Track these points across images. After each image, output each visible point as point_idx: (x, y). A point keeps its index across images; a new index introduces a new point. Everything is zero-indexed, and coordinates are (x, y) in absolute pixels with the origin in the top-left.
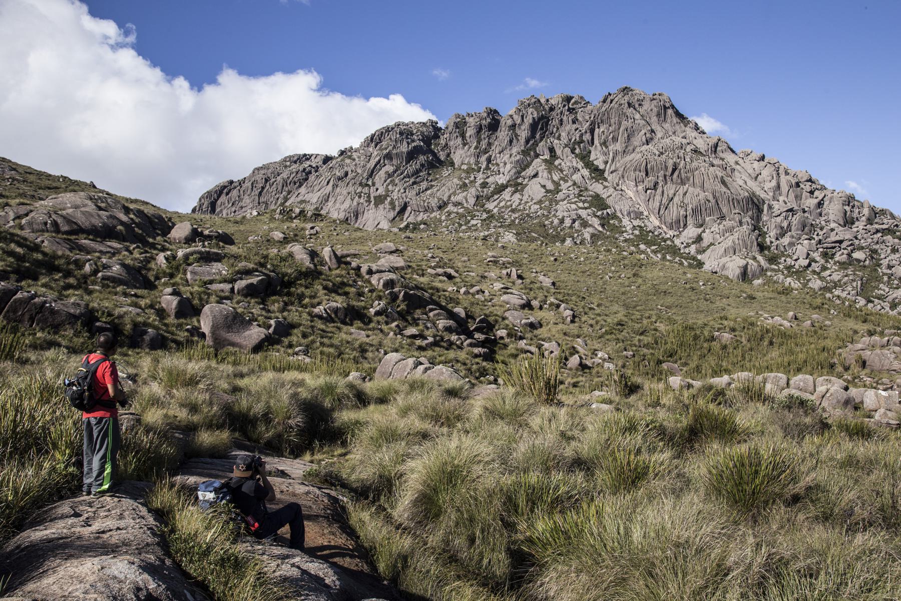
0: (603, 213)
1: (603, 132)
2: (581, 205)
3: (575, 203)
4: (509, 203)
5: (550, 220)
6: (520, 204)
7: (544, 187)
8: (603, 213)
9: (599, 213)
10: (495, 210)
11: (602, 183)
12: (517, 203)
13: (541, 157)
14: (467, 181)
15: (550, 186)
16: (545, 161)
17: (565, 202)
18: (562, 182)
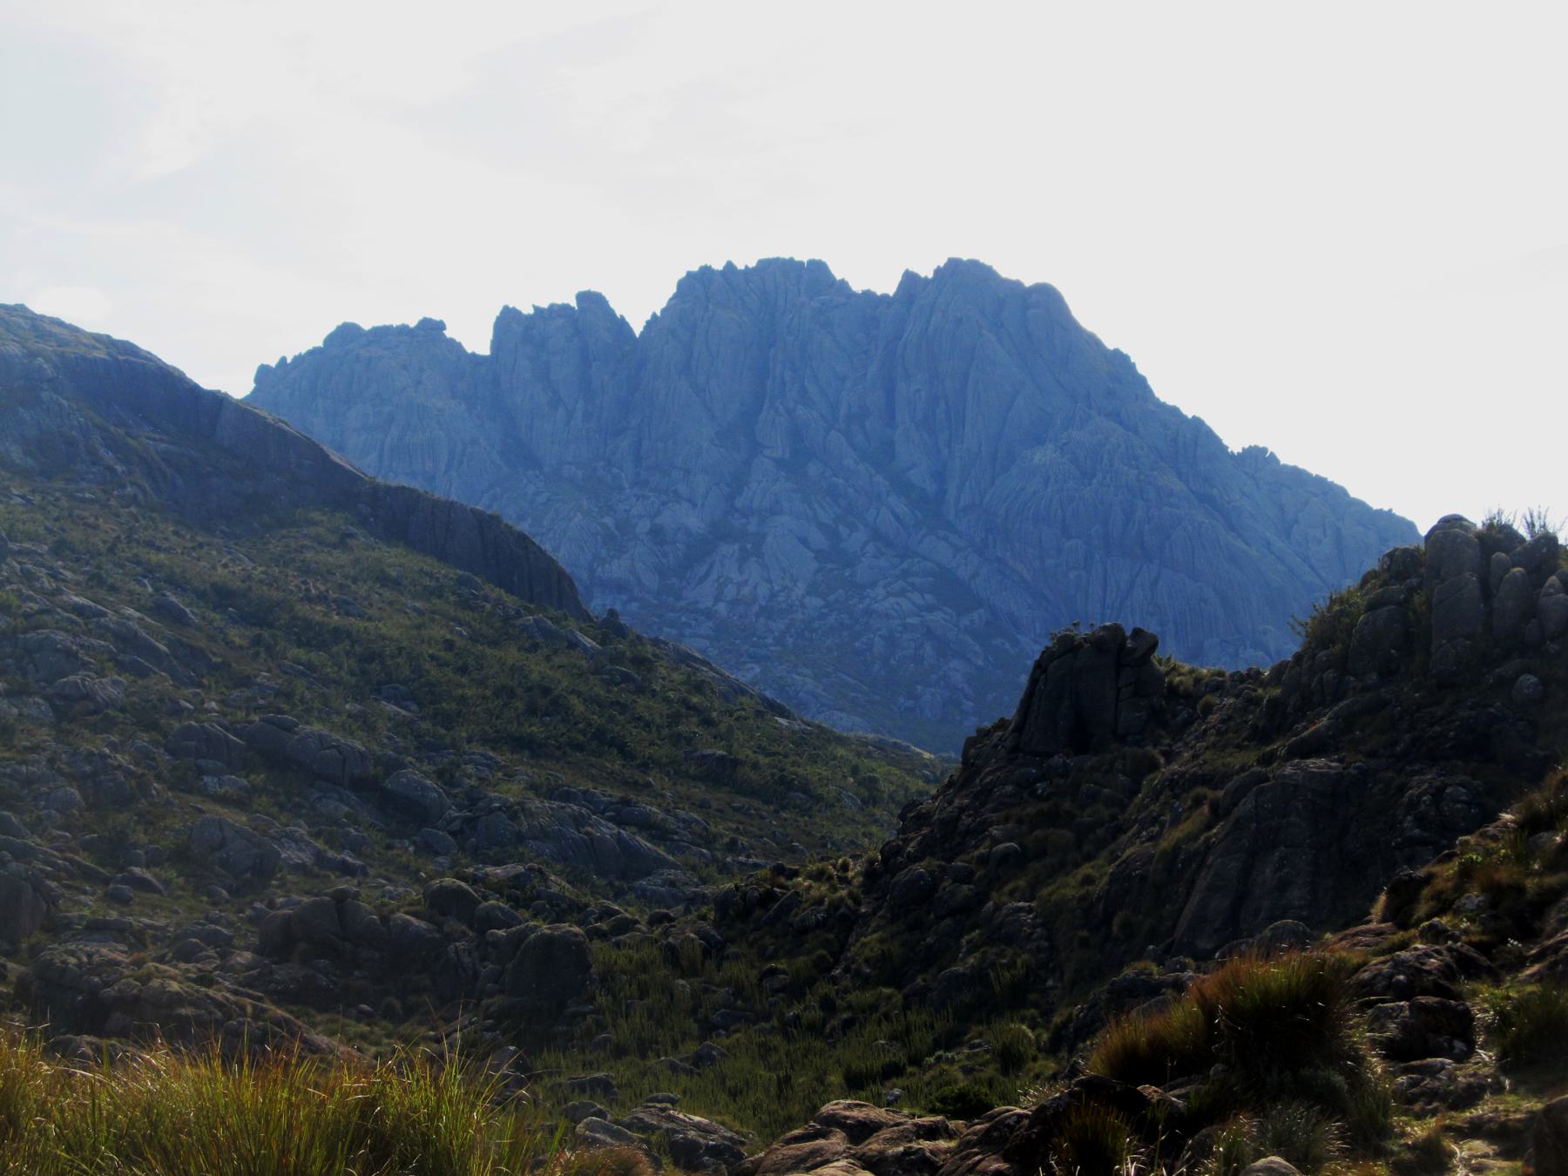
0: (972, 622)
1: (918, 390)
2: (916, 597)
3: (902, 593)
4: (746, 591)
5: (864, 639)
6: (773, 595)
7: (804, 541)
8: (972, 622)
9: (965, 621)
10: (722, 608)
11: (946, 539)
12: (763, 590)
13: (767, 452)
14: (608, 521)
15: (818, 539)
16: (779, 463)
17: (880, 591)
18: (842, 529)
